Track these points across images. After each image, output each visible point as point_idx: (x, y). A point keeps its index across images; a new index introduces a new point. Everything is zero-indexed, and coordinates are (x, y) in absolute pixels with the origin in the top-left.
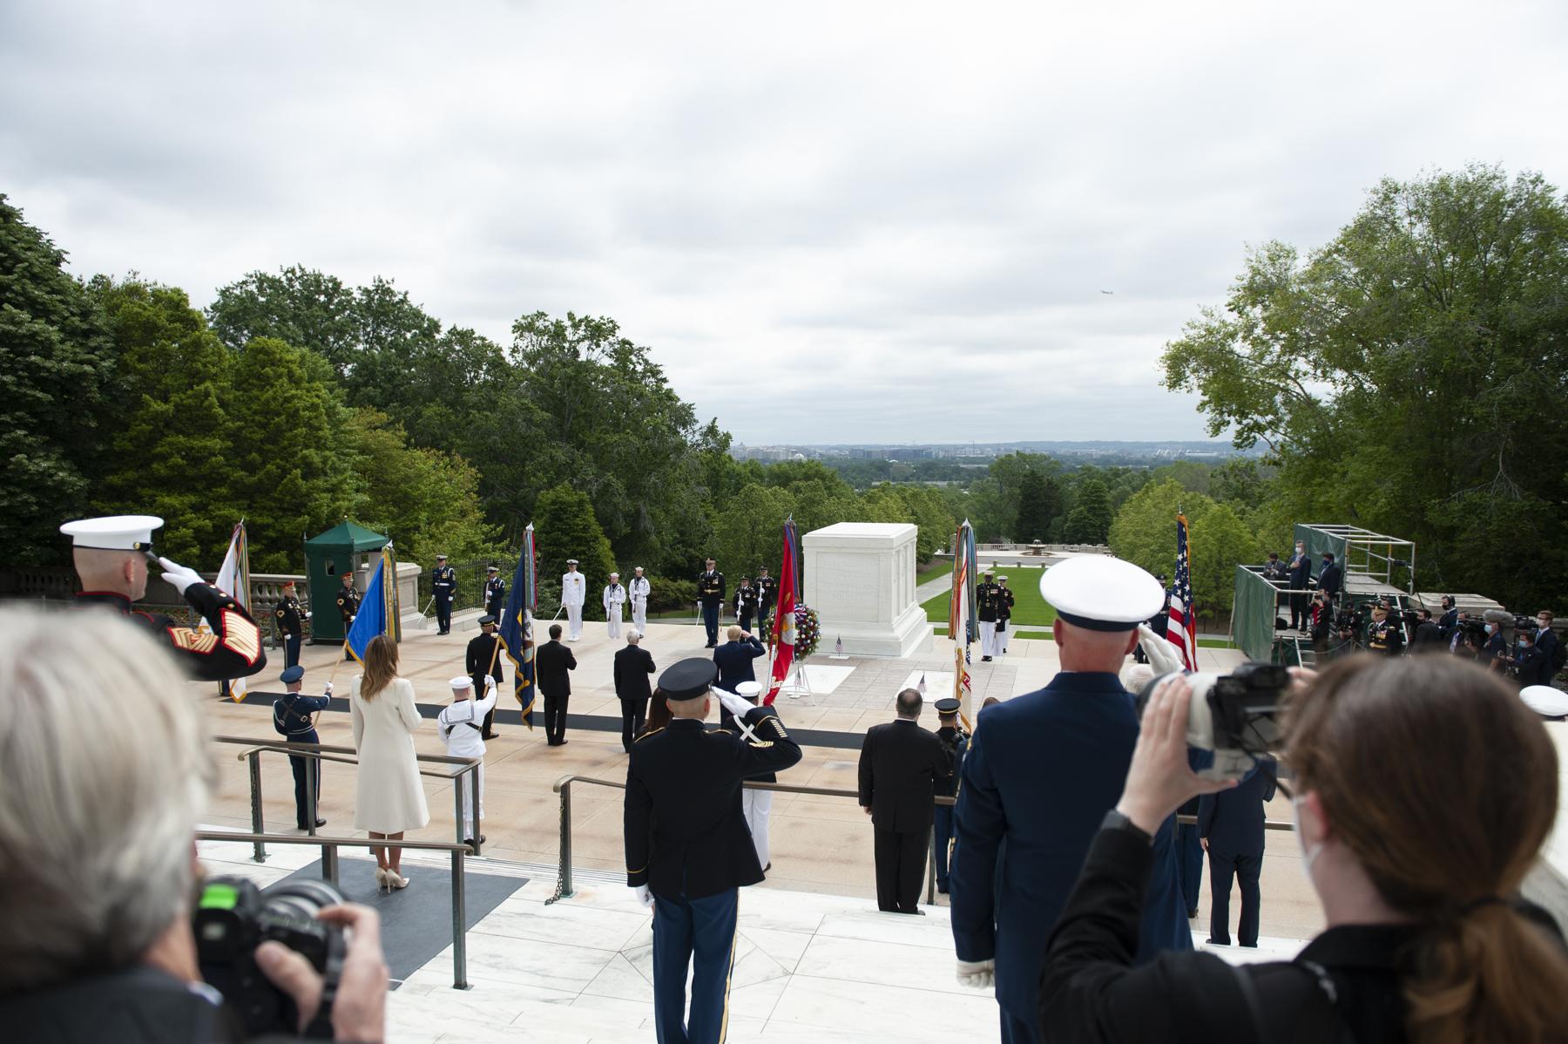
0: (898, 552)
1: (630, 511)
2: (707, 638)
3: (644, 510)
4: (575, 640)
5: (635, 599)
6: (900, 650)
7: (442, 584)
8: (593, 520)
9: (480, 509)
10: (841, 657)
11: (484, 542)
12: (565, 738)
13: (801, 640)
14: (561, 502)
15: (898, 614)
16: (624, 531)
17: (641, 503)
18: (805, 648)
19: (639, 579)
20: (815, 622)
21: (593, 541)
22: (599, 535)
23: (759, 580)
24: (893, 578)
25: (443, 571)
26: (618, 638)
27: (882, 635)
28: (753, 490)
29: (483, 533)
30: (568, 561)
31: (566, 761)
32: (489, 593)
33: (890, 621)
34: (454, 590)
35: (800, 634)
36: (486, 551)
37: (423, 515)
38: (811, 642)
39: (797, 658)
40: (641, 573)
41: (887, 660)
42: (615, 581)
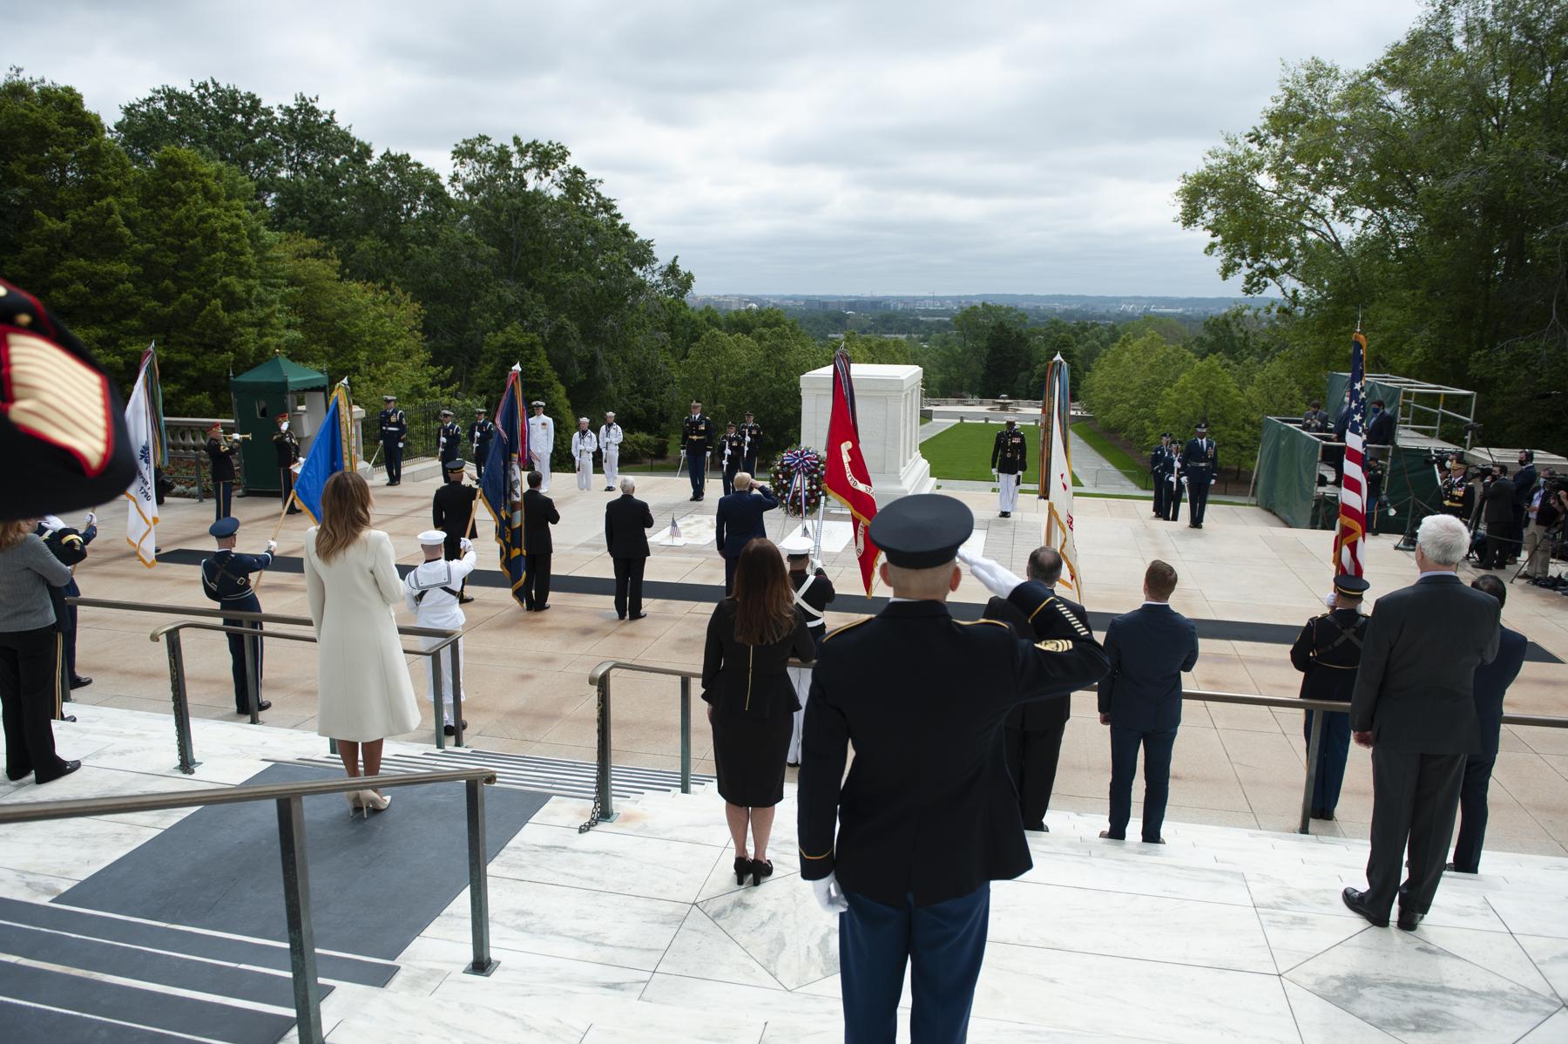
3: (600, 357)
5: (607, 448)
7: (390, 429)
8: (546, 364)
10: (843, 512)
11: (431, 385)
12: (548, 603)
13: (811, 491)
16: (580, 378)
17: (597, 348)
19: (610, 425)
21: (548, 387)
23: (746, 428)
25: (392, 414)
28: (716, 335)
29: (430, 376)
30: (534, 403)
32: (443, 440)
33: (897, 472)
35: (811, 484)
37: (363, 355)
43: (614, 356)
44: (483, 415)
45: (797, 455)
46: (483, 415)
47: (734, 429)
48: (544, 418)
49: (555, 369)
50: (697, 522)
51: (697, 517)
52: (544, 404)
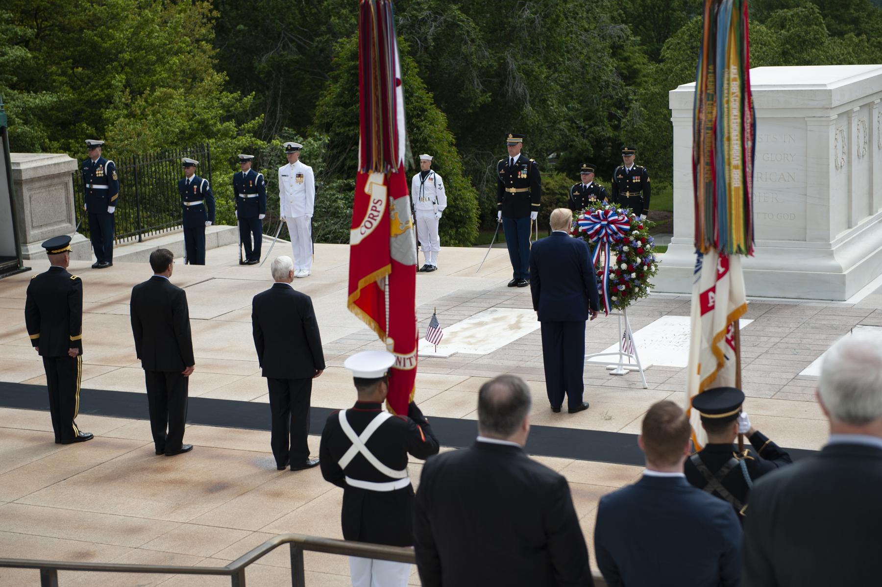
1: (491, 66)
3: (512, 65)
6: (844, 292)
7: (95, 187)
9: (219, 69)
11: (224, 119)
16: (481, 99)
18: (627, 286)
19: (424, 175)
21: (419, 116)
25: (98, 165)
27: (813, 263)
29: (223, 106)
34: (116, 196)
35: (619, 262)
36: (225, 134)
37: (119, 80)
38: (638, 277)
39: (612, 304)
40: (429, 164)
44: (249, 164)
45: (597, 217)
46: (249, 164)
48: (301, 167)
49: (429, 90)
50: (496, 320)
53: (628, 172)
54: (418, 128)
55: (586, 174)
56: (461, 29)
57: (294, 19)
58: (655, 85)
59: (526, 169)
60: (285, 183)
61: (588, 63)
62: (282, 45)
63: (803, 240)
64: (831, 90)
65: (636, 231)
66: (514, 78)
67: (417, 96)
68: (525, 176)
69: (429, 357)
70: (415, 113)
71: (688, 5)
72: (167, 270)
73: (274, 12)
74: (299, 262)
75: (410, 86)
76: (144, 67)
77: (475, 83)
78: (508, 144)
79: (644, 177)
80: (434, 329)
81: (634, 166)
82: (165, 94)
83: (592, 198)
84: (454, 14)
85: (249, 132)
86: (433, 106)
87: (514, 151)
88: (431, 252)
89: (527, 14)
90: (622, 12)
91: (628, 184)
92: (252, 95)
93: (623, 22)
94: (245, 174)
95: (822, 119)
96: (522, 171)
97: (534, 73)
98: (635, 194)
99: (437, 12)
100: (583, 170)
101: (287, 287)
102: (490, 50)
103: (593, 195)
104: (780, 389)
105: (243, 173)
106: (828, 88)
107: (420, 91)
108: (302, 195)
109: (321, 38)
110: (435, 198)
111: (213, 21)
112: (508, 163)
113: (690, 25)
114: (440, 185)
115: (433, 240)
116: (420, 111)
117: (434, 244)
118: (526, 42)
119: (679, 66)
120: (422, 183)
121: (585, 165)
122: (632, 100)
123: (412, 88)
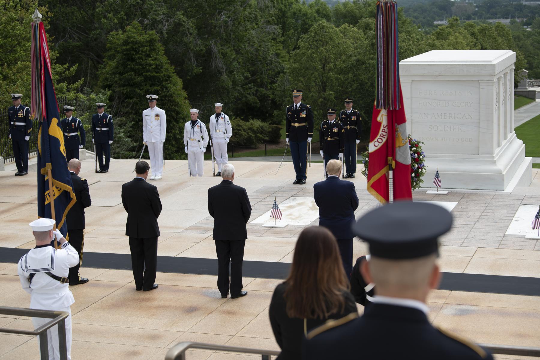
0: (499, 79)
1: (202, 50)
2: (295, 174)
3: (215, 50)
4: (157, 178)
6: (503, 185)
7: (18, 124)
8: (164, 59)
10: (439, 192)
12: (156, 283)
14: (133, 42)
15: (499, 146)
17: (212, 43)
19: (218, 116)
20: (419, 154)
21: (166, 80)
22: (172, 75)
24: (495, 106)
25: (19, 110)
26: (200, 175)
28: (323, 27)
30: (148, 96)
31: (158, 307)
33: (491, 153)
34: (31, 130)
38: (416, 176)
40: (221, 109)
41: (490, 195)
42: (195, 117)
43: (228, 50)
44: (103, 109)
47: (334, 116)
49: (172, 64)
50: (299, 204)
51: (300, 200)
52: (157, 97)
53: (348, 114)
54: (167, 88)
55: (332, 115)
56: (184, 27)
57: (76, 19)
58: (295, 63)
59: (305, 111)
60: (147, 120)
61: (259, 49)
62: (68, 36)
63: (477, 154)
64: (495, 64)
65: (414, 148)
66: (216, 57)
67: (164, 68)
68: (304, 116)
69: (272, 227)
70: (164, 78)
71: (296, 15)
72: (145, 174)
73: (64, 15)
74: (155, 170)
75: (160, 62)
76: (10, 49)
77: (193, 60)
78: (294, 96)
79: (358, 117)
80: (277, 210)
81: (352, 110)
82: (25, 66)
83: (335, 130)
84: (179, 17)
85: (74, 90)
86: (175, 74)
87: (298, 100)
88: (222, 164)
89: (223, 18)
90: (275, 18)
91: (348, 121)
92: (76, 66)
93: (275, 24)
94: (100, 116)
95: (489, 81)
96: (303, 113)
97: (228, 55)
98: (353, 127)
99: (168, 16)
100: (329, 113)
101: (231, 183)
102: (200, 40)
103: (336, 128)
104: (500, 243)
105: (99, 115)
106: (493, 63)
107: (167, 65)
108: (159, 127)
109: (95, 32)
110: (225, 130)
111: (49, 19)
112: (294, 108)
113: (315, 26)
114: (228, 122)
115: (224, 157)
116: (167, 77)
117: (224, 159)
118: (223, 35)
119: (310, 51)
120: (217, 121)
121: (330, 110)
122: (286, 72)
123: (161, 63)
